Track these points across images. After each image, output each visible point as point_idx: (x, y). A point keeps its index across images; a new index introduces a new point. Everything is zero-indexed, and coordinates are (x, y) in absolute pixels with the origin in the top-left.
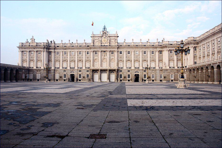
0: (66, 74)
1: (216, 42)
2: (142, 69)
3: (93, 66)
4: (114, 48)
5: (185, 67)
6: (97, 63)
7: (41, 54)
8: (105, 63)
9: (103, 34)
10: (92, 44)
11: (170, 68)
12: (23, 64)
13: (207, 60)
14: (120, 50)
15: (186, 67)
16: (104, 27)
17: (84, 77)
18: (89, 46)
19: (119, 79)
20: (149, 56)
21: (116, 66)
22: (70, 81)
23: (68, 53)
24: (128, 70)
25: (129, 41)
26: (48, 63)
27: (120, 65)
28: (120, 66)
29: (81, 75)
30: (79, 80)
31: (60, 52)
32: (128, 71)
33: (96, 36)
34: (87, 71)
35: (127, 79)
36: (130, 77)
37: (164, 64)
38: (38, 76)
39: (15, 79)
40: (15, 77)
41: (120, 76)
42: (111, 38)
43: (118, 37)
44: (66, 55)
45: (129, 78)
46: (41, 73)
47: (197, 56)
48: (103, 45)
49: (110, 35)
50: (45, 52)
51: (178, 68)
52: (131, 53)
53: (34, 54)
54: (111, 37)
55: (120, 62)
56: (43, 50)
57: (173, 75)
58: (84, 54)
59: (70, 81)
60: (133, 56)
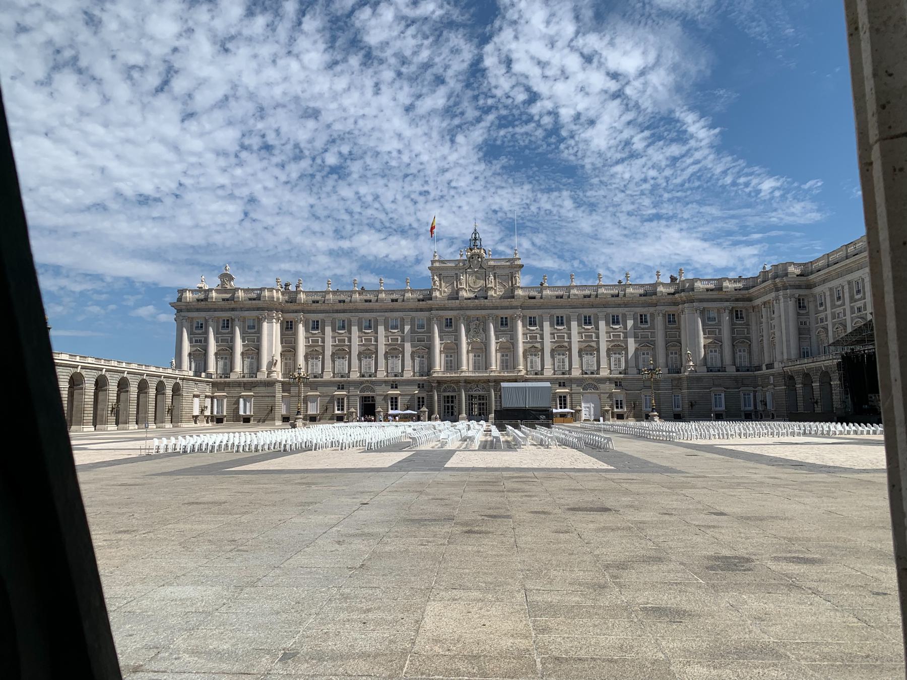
6: (451, 356)
11: (709, 370)
15: (770, 366)
24: (557, 379)
27: (532, 362)
39: (168, 418)
42: (498, 271)
47: (809, 330)
51: (738, 370)
54: (498, 267)
57: (723, 395)
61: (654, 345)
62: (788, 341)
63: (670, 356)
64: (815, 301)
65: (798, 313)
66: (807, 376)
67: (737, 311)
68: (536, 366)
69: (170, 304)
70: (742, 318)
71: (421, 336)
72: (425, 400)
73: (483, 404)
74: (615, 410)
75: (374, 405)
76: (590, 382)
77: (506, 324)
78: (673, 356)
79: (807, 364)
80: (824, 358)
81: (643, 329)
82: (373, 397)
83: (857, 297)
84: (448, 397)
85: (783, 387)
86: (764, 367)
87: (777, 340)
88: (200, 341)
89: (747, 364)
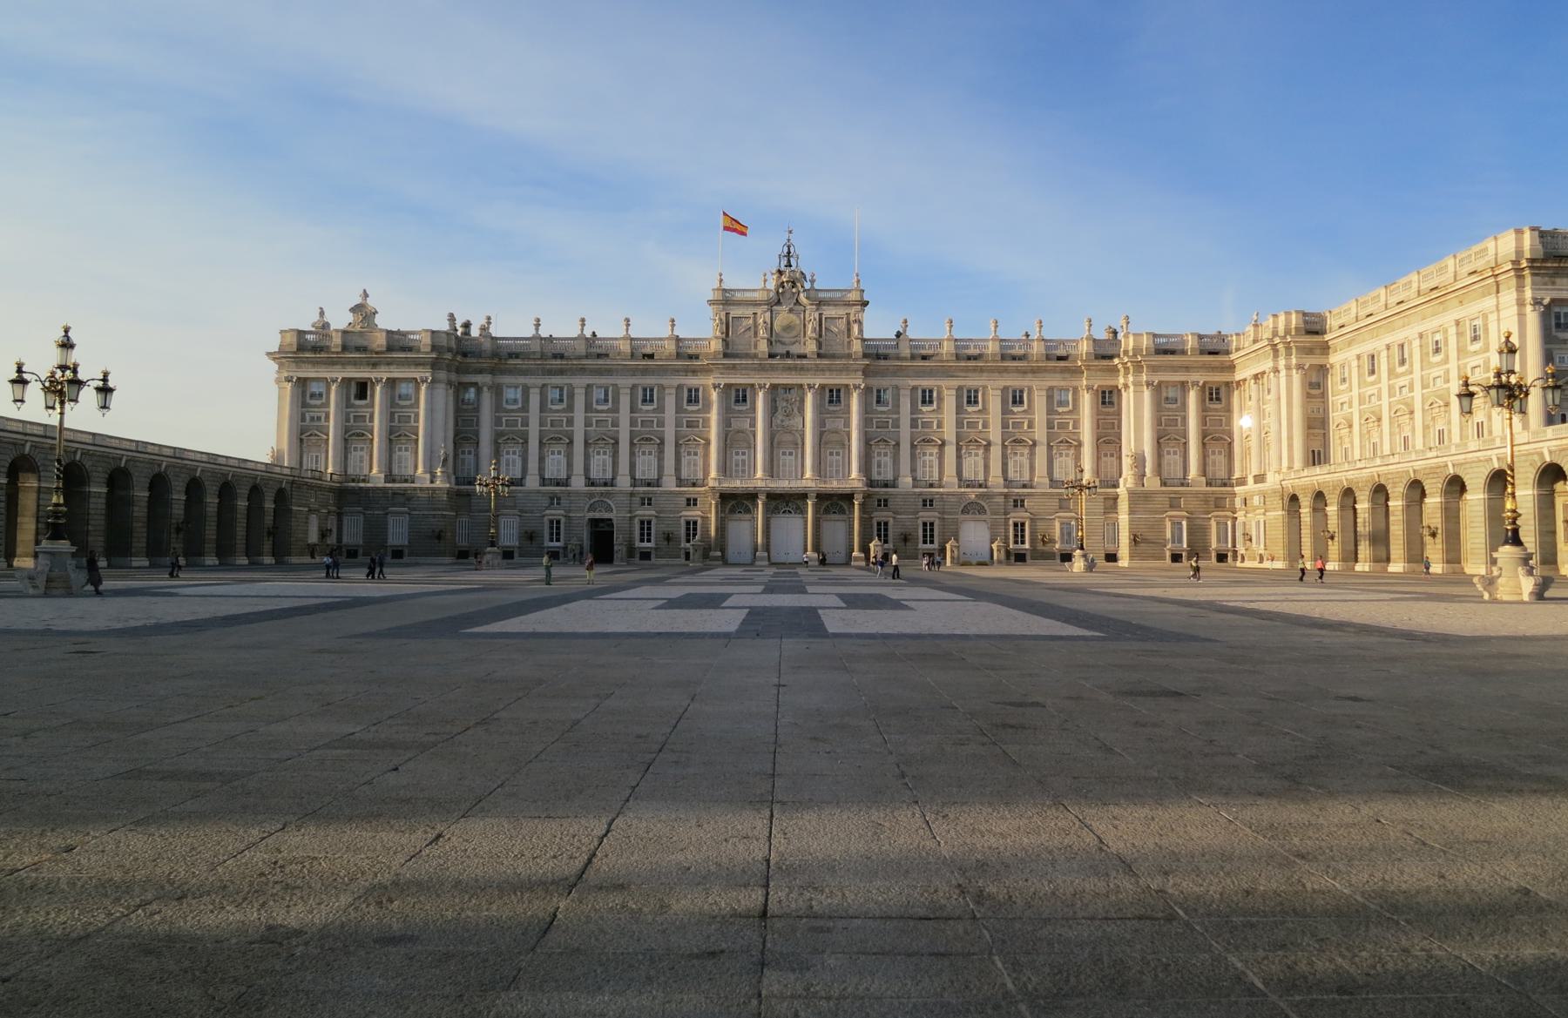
0: (563, 520)
1: (1452, 340)
2: (1006, 490)
4: (845, 370)
5: (1256, 482)
6: (744, 454)
9: (780, 291)
11: (1164, 484)
12: (301, 457)
14: (877, 382)
15: (1260, 479)
16: (786, 250)
17: (668, 538)
23: (571, 396)
24: (921, 494)
27: (879, 466)
28: (879, 473)
29: (649, 523)
31: (526, 391)
32: (925, 505)
33: (738, 296)
34: (689, 500)
35: (921, 545)
37: (1127, 462)
40: (269, 533)
41: (879, 530)
42: (829, 312)
43: (865, 304)
45: (932, 542)
46: (415, 509)
48: (780, 349)
49: (821, 295)
51: (1209, 484)
55: (882, 448)
56: (428, 375)
57: (1184, 523)
58: (670, 402)
61: (1079, 437)
62: (1290, 438)
63: (1104, 459)
65: (1308, 393)
66: (1319, 496)
67: (1211, 389)
68: (886, 472)
69: (269, 354)
70: (1218, 399)
77: (839, 401)
78: (1109, 459)
79: (1319, 476)
80: (1346, 467)
82: (611, 520)
83: (1401, 370)
85: (1280, 513)
86: (1250, 480)
87: (1272, 437)
88: (319, 419)
89: (1222, 474)
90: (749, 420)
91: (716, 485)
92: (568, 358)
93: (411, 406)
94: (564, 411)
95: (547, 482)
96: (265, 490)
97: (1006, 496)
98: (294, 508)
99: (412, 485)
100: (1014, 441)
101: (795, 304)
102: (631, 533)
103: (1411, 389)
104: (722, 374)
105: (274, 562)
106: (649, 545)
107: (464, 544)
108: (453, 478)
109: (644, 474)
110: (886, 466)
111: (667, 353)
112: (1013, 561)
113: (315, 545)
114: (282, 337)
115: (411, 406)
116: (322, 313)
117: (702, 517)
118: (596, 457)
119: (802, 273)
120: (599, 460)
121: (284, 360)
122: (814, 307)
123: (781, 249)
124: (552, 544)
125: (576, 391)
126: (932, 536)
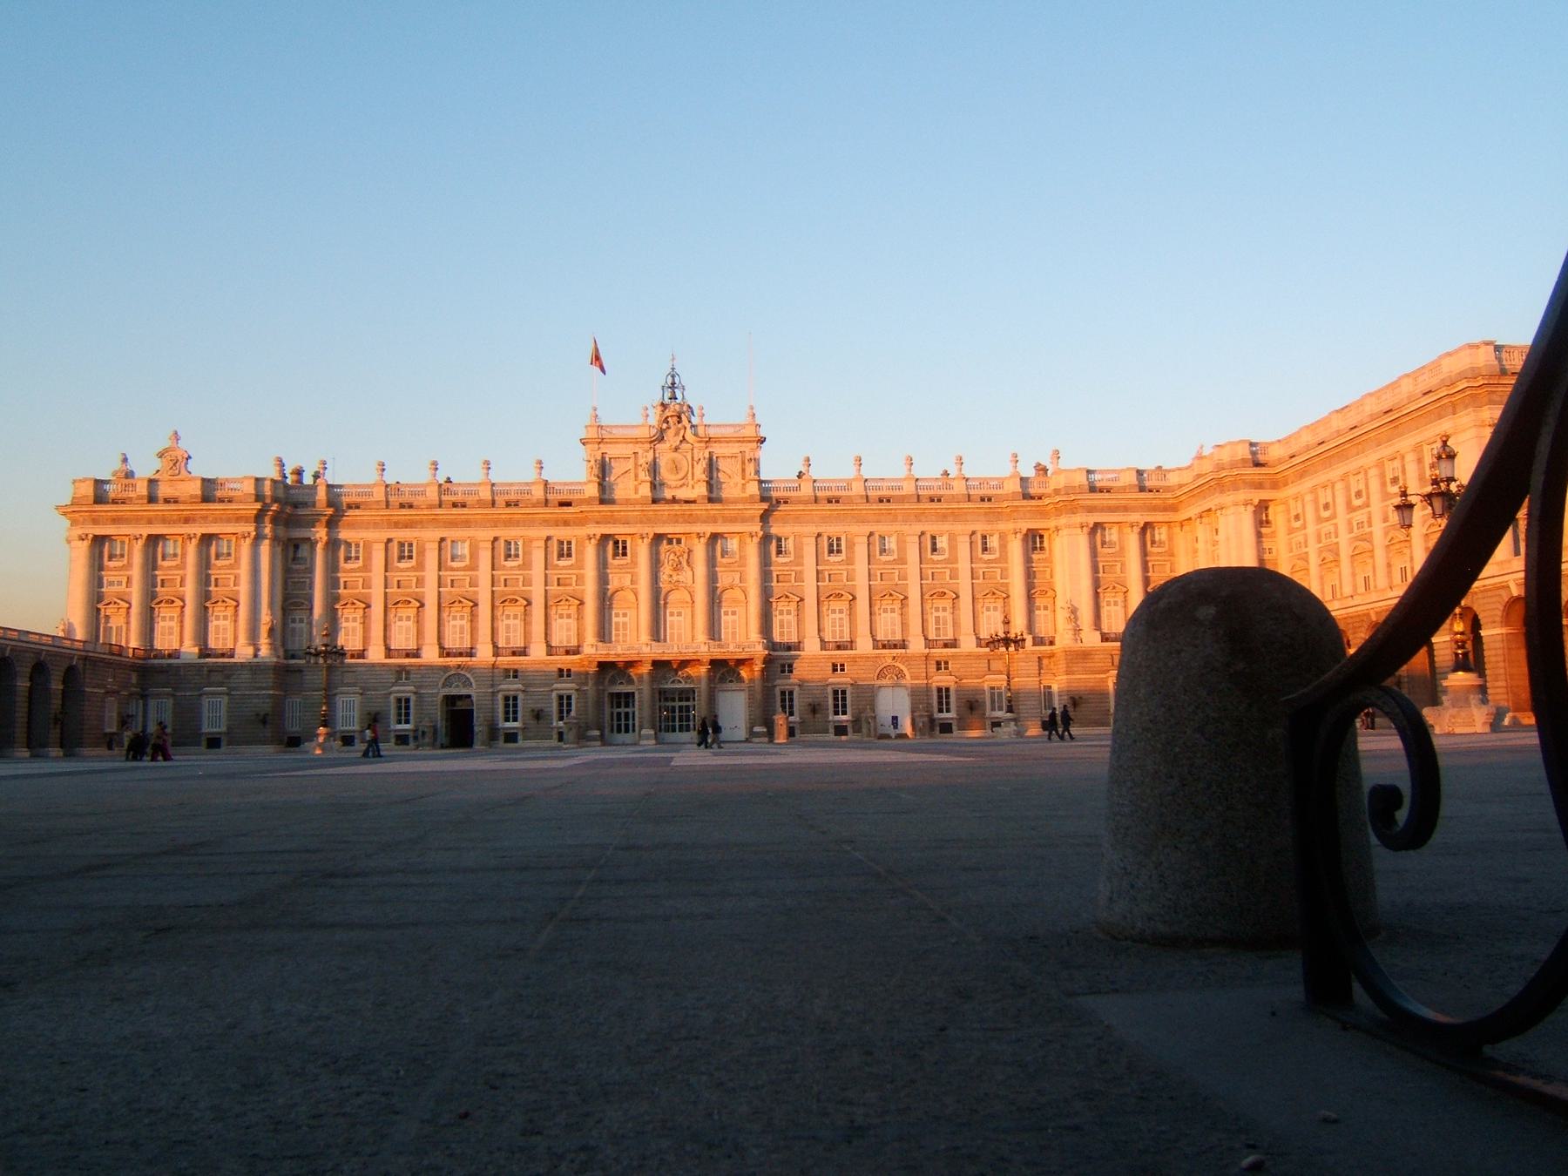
0: (413, 698)
3: (603, 634)
6: (625, 615)
7: (237, 560)
8: (679, 614)
10: (592, 491)
13: (1355, 587)
16: (670, 380)
18: (568, 504)
19: (780, 720)
20: (964, 565)
21: (754, 635)
22: (442, 747)
24: (831, 657)
25: (832, 469)
26: (284, 624)
27: (782, 626)
30: (502, 738)
32: (835, 670)
33: (618, 433)
35: (831, 717)
36: (849, 710)
38: (214, 714)
39: (55, 733)
40: (56, 720)
41: (783, 700)
43: (762, 440)
44: (413, 562)
46: (235, 689)
49: (712, 432)
50: (265, 547)
52: (851, 545)
53: (184, 555)
54: (718, 440)
58: (538, 557)
59: (438, 743)
60: (861, 567)
61: (1008, 590)
64: (1288, 511)
69: (57, 508)
71: (563, 574)
72: (573, 702)
73: (688, 707)
74: (937, 715)
75: (472, 710)
76: (889, 661)
81: (989, 561)
82: (469, 696)
83: (1357, 502)
84: (619, 695)
90: (630, 576)
91: (593, 651)
92: (418, 508)
93: (231, 567)
94: (413, 569)
95: (392, 653)
96: (51, 667)
97: (927, 657)
98: (87, 689)
99: (232, 660)
100: (933, 593)
101: (681, 441)
102: (493, 711)
103: (1370, 525)
104: (598, 523)
105: (61, 754)
106: (515, 724)
107: (294, 729)
108: (281, 653)
109: (508, 642)
110: (789, 623)
111: (534, 499)
112: (938, 733)
113: (113, 734)
114: (76, 488)
115: (231, 567)
116: (125, 460)
117: (577, 690)
118: (452, 623)
119: (689, 407)
120: (454, 626)
121: (77, 515)
122: (703, 445)
123: (662, 379)
124: (400, 727)
125: (428, 546)
126: (844, 706)
